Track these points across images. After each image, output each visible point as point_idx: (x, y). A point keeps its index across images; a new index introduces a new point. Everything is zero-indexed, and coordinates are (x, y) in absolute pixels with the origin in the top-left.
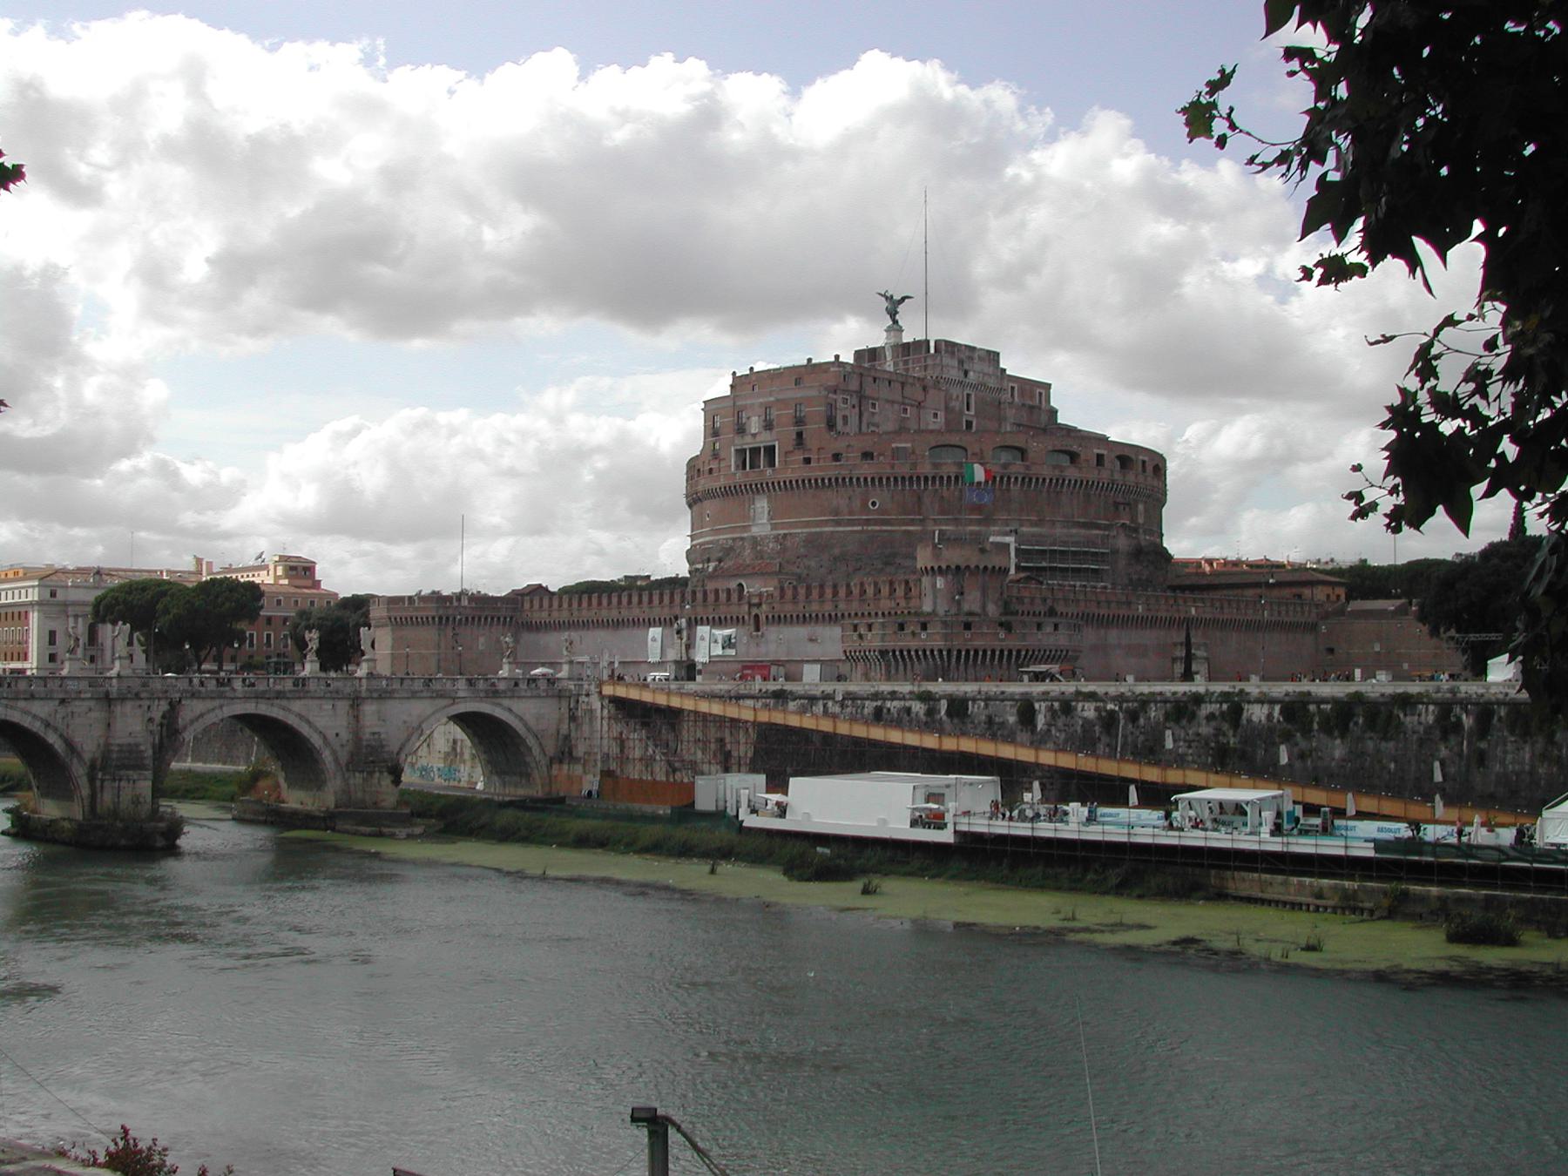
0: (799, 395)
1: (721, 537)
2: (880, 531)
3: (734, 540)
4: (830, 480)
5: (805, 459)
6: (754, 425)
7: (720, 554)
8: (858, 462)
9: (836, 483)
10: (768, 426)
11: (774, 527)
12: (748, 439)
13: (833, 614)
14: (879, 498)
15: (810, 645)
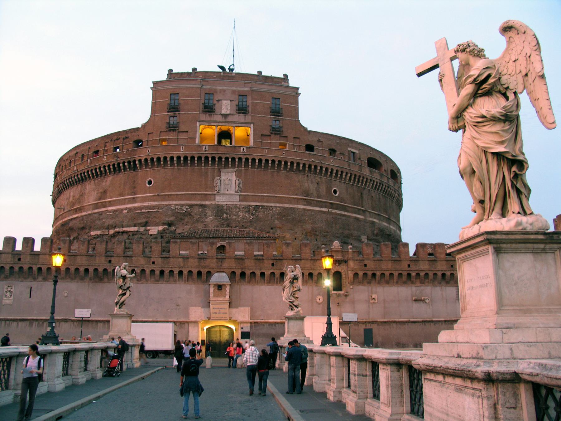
0: (276, 91)
1: (174, 202)
2: (341, 215)
3: (191, 206)
4: (304, 165)
5: (280, 142)
6: (226, 107)
7: (172, 219)
8: (327, 155)
9: (311, 169)
10: (242, 110)
11: (244, 198)
12: (218, 118)
13: (448, 274)
14: (339, 187)
15: (416, 305)
